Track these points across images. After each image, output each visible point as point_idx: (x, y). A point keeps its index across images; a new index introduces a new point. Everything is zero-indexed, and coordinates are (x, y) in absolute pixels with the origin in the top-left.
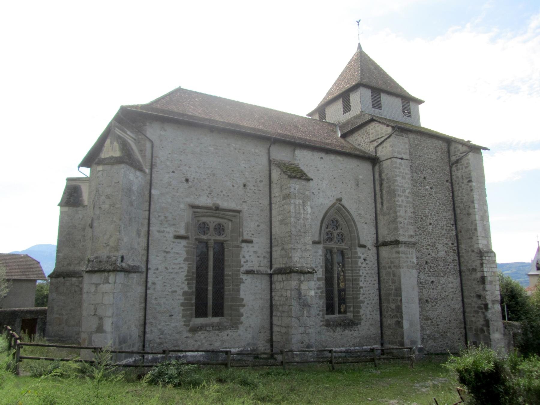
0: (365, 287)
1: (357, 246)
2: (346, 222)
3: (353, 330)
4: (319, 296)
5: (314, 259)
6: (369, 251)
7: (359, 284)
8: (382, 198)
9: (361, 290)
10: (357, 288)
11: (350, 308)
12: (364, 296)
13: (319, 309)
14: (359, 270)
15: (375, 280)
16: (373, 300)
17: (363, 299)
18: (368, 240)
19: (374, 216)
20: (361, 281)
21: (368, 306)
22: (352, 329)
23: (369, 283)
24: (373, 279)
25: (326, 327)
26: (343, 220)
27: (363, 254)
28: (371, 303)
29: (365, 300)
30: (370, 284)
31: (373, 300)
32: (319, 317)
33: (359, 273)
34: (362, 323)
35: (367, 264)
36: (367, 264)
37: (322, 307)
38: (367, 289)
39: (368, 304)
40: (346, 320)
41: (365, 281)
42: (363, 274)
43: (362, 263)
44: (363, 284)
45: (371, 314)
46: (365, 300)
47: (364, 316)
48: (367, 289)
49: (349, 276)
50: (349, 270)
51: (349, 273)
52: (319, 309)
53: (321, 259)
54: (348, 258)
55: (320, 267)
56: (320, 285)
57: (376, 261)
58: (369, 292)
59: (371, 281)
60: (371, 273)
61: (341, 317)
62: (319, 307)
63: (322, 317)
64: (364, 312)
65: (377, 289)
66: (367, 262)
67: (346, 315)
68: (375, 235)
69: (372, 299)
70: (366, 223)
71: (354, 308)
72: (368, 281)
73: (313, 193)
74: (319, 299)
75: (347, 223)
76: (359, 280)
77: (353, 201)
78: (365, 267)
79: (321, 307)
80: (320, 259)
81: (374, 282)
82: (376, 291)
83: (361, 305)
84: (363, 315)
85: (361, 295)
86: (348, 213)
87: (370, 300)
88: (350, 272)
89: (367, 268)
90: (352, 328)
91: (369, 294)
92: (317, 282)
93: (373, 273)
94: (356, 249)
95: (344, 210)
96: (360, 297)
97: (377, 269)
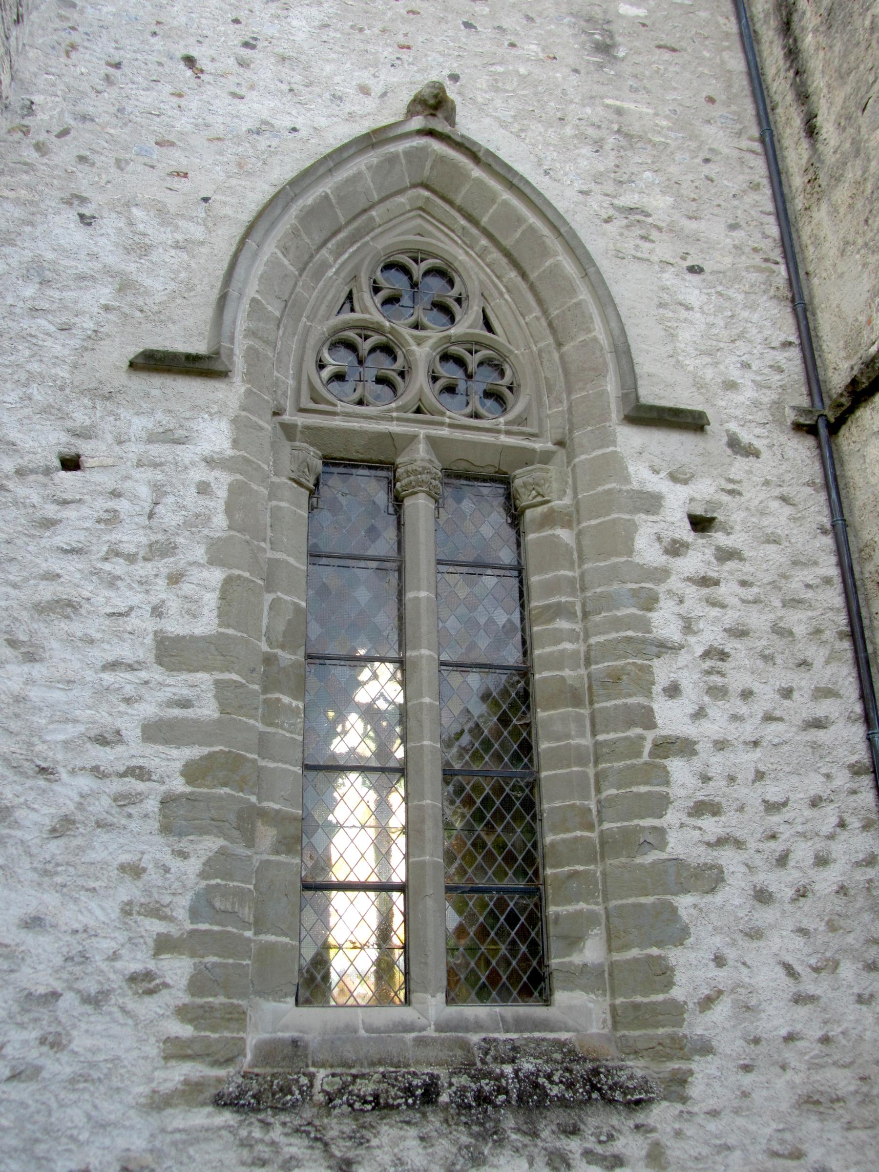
0: (721, 745)
1: (615, 416)
2: (515, 264)
3: (588, 1155)
4: (167, 801)
5: (144, 491)
6: (739, 466)
7: (648, 719)
8: (803, 96)
9: (676, 767)
10: (634, 747)
11: (574, 942)
12: (711, 826)
13: (157, 927)
14: (650, 602)
15: (823, 693)
16: (822, 861)
17: (699, 855)
18: (731, 386)
19: (774, 231)
20: (673, 691)
21: (766, 916)
22: (574, 1145)
23: (759, 707)
24: (803, 682)
25: (227, 1117)
26: (495, 255)
27: (676, 478)
28: (802, 894)
29: (728, 858)
30: (769, 718)
31: (822, 861)
32: (147, 1008)
33: (646, 626)
34: (696, 1089)
35: (726, 555)
36: (726, 555)
37: (194, 914)
38: (749, 759)
39: (762, 896)
40: (514, 1053)
41: (718, 692)
42: (688, 626)
43: (676, 549)
44: (700, 714)
45: (799, 999)
46: (728, 858)
47: (721, 1011)
48: (749, 759)
49: (558, 661)
50: (559, 611)
51: (557, 637)
52: (157, 927)
53: (222, 493)
54: (550, 520)
55: (199, 553)
56: (185, 704)
57: (828, 541)
58: (773, 792)
59: (787, 693)
60: (781, 631)
61: (478, 1026)
62: (156, 912)
63: (183, 1013)
64: (722, 976)
65: (856, 771)
66: (719, 538)
67: (537, 1011)
68: (795, 353)
69: (803, 852)
70: (695, 270)
71: (612, 942)
72: (747, 695)
73: (190, 61)
74: (166, 829)
75: (524, 275)
76: (644, 683)
77: (569, 131)
78: (705, 582)
79: (181, 907)
80: (204, 489)
81: (826, 708)
82: (842, 779)
83: (685, 903)
84: (707, 1003)
85: (672, 817)
86: (488, 168)
87: (782, 860)
88: (563, 624)
89: (727, 591)
90: (573, 1131)
91: (772, 807)
92: (156, 674)
93: (800, 630)
94: (607, 439)
95: (477, 172)
96: (660, 832)
97: (834, 597)
